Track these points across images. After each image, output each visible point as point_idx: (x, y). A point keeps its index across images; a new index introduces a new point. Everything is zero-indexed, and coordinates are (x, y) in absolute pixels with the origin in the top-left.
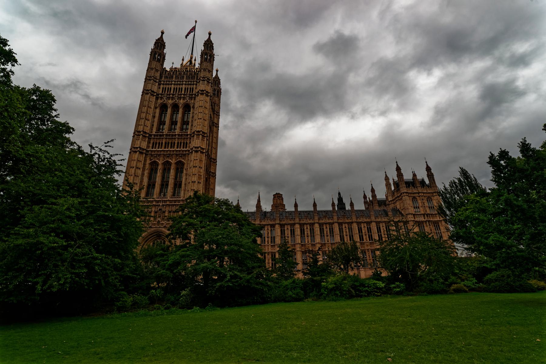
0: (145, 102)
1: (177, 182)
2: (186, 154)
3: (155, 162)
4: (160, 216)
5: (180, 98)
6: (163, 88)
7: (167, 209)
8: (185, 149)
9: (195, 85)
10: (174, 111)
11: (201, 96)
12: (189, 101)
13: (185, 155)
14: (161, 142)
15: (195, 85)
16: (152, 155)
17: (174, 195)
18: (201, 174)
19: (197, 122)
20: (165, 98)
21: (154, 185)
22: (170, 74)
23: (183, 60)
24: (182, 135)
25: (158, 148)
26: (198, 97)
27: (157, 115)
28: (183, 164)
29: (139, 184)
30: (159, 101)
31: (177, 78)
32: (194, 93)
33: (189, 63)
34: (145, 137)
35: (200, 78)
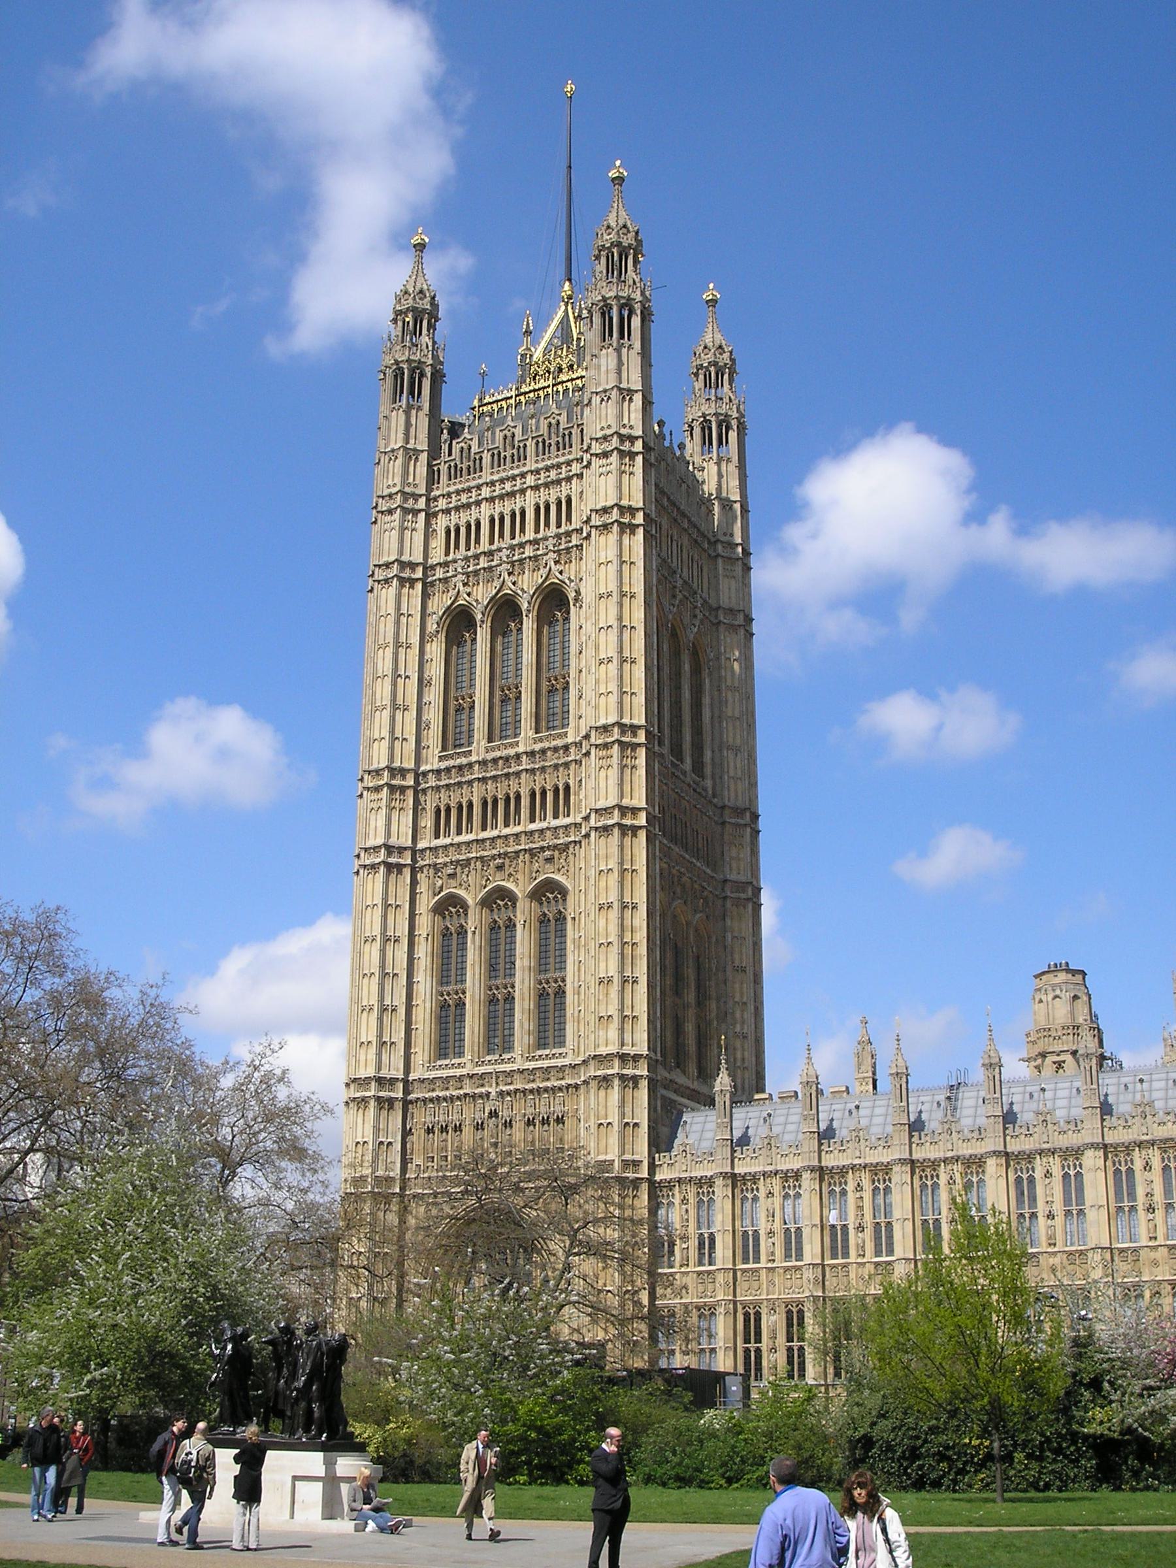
0: (382, 626)
1: (548, 982)
2: (567, 845)
7: (519, 1110)
8: (562, 821)
11: (603, 538)
17: (542, 1043)
19: (597, 682)
21: (461, 1005)
22: (470, 446)
24: (543, 752)
25: (459, 833)
26: (592, 549)
27: (436, 671)
28: (563, 892)
29: (402, 1011)
30: (440, 603)
31: (498, 460)
32: (573, 526)
33: (559, 334)
34: (403, 789)
35: (589, 447)
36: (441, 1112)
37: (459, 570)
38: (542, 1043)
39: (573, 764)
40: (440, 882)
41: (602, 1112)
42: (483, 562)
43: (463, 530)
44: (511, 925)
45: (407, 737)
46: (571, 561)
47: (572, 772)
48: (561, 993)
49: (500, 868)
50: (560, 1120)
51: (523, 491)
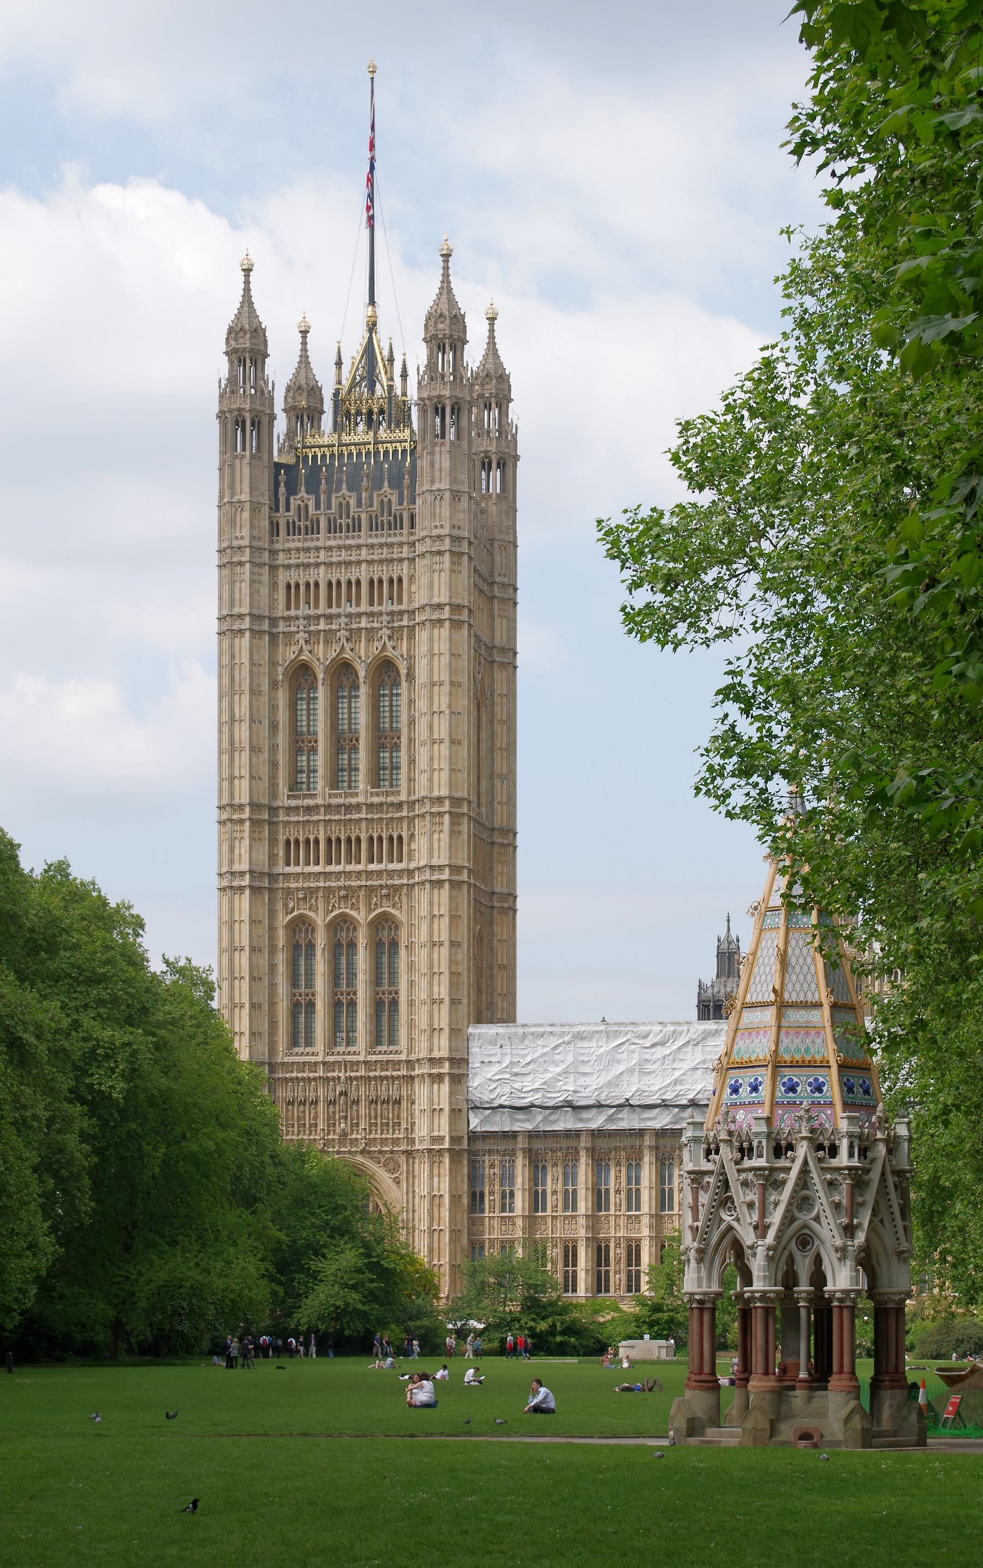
1: (383, 994)
3: (302, 919)
4: (346, 1117)
5: (353, 635)
6: (288, 586)
9: (406, 564)
10: (340, 687)
12: (389, 644)
13: (397, 889)
14: (312, 838)
15: (406, 564)
16: (288, 891)
18: (460, 969)
20: (302, 636)
23: (339, 364)
24: (381, 804)
27: (283, 716)
31: (333, 528)
36: (300, 1089)
37: (301, 627)
38: (378, 1042)
39: (406, 820)
40: (291, 905)
41: (436, 1100)
42: (322, 626)
43: (302, 588)
44: (352, 945)
45: (262, 776)
46: (402, 639)
47: (405, 826)
48: (394, 1003)
49: (345, 897)
50: (398, 1102)
51: (359, 563)
